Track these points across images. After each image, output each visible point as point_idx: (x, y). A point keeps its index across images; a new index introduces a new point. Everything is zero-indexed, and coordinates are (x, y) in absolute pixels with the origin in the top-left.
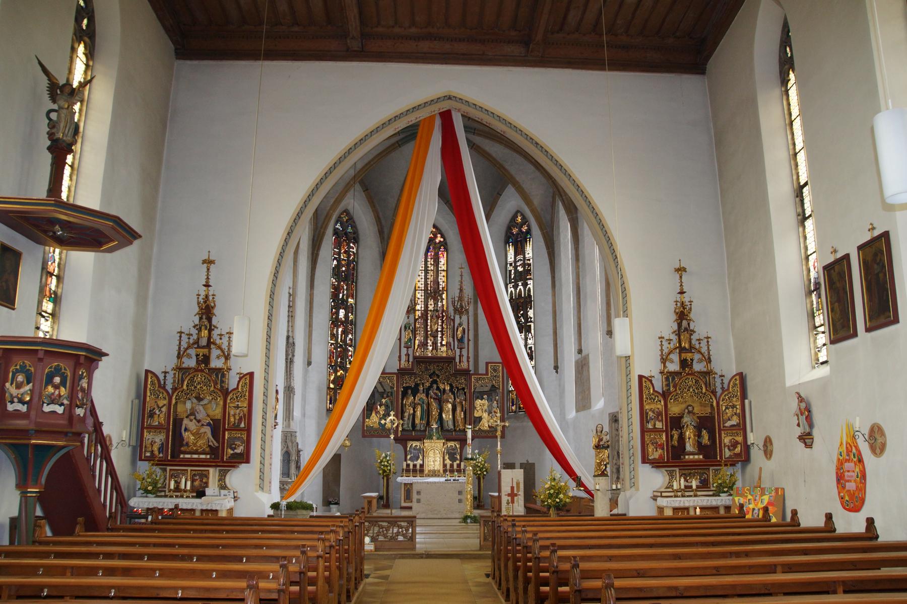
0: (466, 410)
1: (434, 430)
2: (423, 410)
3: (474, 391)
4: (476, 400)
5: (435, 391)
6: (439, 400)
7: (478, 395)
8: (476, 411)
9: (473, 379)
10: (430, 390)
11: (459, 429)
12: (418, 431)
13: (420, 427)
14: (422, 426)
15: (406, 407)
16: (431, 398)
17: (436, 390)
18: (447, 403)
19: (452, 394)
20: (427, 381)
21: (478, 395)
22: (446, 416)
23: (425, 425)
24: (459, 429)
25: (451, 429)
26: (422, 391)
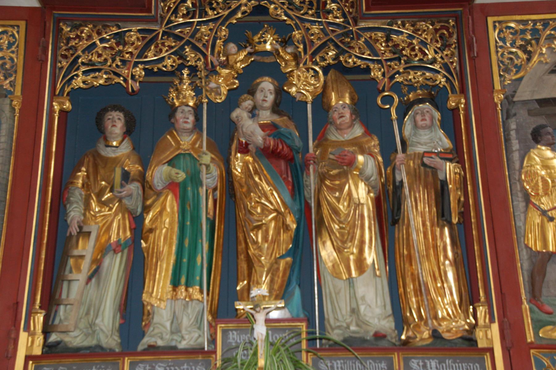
0: (464, 215)
1: (260, 330)
2: (196, 219)
3: (509, 100)
4: (525, 152)
5: (266, 117)
6: (290, 160)
7: (541, 121)
8: (536, 219)
9: (494, 35)
10: (237, 105)
11: (436, 334)
12: (152, 350)
13: (176, 330)
14: (185, 322)
15: (87, 206)
16: (244, 149)
17: (276, 108)
18: (344, 175)
19: (368, 132)
20: (224, 65)
21: (541, 121)
22: (339, 250)
23: (207, 317)
24: (436, 334)
25: (379, 336)
26: (191, 118)
